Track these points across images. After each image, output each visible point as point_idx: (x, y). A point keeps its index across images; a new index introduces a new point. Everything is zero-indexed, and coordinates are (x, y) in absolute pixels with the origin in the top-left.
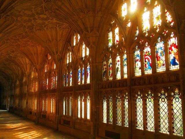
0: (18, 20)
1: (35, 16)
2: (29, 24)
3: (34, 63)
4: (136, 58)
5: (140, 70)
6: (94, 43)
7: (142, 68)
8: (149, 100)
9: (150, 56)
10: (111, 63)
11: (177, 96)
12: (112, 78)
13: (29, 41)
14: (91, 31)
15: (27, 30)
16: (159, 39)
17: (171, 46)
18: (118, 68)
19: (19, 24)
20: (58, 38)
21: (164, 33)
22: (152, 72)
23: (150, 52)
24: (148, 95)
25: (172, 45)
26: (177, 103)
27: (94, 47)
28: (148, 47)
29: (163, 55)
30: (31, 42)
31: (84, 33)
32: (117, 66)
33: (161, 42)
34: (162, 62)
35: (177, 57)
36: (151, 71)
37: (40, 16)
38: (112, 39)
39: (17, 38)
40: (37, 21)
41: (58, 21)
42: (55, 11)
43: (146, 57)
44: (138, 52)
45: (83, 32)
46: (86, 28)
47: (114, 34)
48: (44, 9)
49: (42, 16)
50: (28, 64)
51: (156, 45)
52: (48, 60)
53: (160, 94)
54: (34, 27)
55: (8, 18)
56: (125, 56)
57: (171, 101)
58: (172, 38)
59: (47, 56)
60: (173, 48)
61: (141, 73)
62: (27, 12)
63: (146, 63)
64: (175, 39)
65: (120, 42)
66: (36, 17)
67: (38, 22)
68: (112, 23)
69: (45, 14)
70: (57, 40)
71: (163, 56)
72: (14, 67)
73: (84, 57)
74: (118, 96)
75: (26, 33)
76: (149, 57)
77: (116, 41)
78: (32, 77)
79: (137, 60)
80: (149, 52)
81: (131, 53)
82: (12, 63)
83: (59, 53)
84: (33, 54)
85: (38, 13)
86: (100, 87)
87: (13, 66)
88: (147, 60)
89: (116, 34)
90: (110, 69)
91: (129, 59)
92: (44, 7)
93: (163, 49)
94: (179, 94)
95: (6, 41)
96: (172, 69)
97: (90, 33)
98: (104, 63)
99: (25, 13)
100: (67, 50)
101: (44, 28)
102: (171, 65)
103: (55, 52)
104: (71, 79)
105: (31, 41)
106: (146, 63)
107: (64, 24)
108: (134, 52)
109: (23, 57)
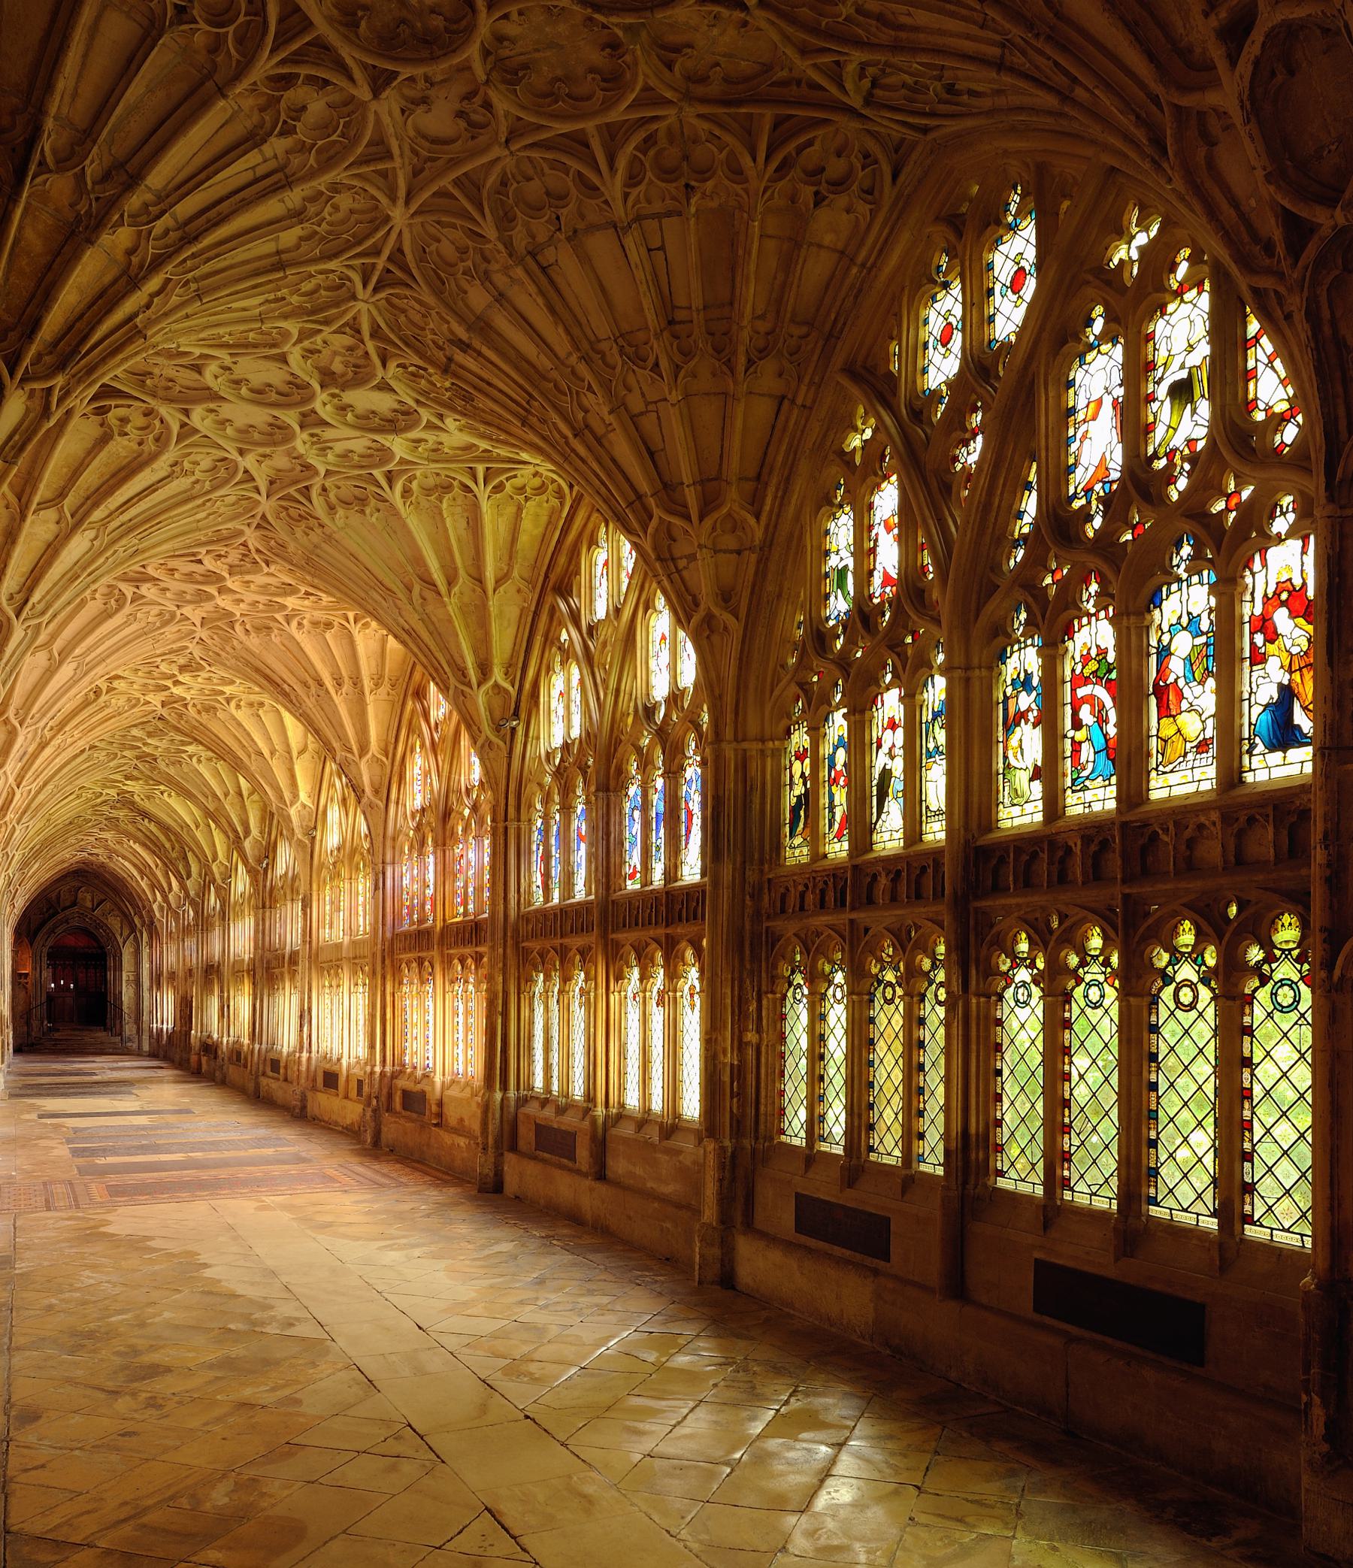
2: (281, 461)
3: (336, 745)
4: (1012, 703)
5: (1037, 787)
6: (726, 597)
7: (1047, 772)
8: (1086, 996)
9: (1109, 686)
10: (841, 737)
11: (1286, 970)
12: (846, 845)
13: (288, 590)
14: (708, 505)
15: (267, 506)
16: (1186, 550)
17: (1272, 601)
18: (886, 774)
19: (206, 463)
20: (490, 575)
21: (1220, 506)
22: (1119, 799)
23: (1111, 657)
24: (1083, 964)
25: (1277, 594)
26: (1286, 1021)
28: (1102, 614)
29: (1207, 672)
30: (307, 593)
32: (880, 761)
33: (1195, 579)
34: (1191, 725)
35: (1307, 688)
36: (1112, 791)
37: (351, 397)
38: (850, 562)
39: (209, 563)
40: (329, 434)
41: (483, 436)
42: (450, 359)
43: (1081, 692)
44: (1026, 659)
45: (651, 517)
46: (668, 488)
47: (863, 528)
48: (371, 346)
49: (363, 399)
50: (300, 753)
51: (1155, 601)
52: (428, 721)
53: (1166, 957)
54: (317, 483)
55: (122, 412)
56: (937, 691)
57: (1238, 1002)
58: (1279, 540)
59: (420, 694)
60: (1281, 618)
61: (1040, 805)
62: (258, 371)
63: (1080, 735)
64: (1304, 552)
65: (910, 581)
66: (322, 404)
67: (339, 448)
68: (855, 442)
69: (384, 387)
70: (480, 580)
71: (1202, 683)
72: (207, 775)
73: (667, 701)
74: (882, 969)
75: (263, 524)
76: (1101, 692)
77: (877, 579)
78: (332, 838)
79: (1021, 716)
80: (1103, 652)
81: (975, 661)
82: (191, 749)
83: (498, 675)
84: (329, 683)
85: (328, 378)
87: (201, 768)
88: (1086, 714)
89: (880, 530)
90: (834, 782)
91: (958, 711)
93: (1205, 625)
94: (1300, 960)
95: (128, 590)
96: (1262, 776)
97: (695, 517)
98: (795, 738)
100: (554, 649)
101: (387, 493)
102: (1260, 748)
104: (581, 855)
105: (303, 589)
106: (1080, 735)
107: (525, 456)
108: (1002, 658)
109: (261, 704)
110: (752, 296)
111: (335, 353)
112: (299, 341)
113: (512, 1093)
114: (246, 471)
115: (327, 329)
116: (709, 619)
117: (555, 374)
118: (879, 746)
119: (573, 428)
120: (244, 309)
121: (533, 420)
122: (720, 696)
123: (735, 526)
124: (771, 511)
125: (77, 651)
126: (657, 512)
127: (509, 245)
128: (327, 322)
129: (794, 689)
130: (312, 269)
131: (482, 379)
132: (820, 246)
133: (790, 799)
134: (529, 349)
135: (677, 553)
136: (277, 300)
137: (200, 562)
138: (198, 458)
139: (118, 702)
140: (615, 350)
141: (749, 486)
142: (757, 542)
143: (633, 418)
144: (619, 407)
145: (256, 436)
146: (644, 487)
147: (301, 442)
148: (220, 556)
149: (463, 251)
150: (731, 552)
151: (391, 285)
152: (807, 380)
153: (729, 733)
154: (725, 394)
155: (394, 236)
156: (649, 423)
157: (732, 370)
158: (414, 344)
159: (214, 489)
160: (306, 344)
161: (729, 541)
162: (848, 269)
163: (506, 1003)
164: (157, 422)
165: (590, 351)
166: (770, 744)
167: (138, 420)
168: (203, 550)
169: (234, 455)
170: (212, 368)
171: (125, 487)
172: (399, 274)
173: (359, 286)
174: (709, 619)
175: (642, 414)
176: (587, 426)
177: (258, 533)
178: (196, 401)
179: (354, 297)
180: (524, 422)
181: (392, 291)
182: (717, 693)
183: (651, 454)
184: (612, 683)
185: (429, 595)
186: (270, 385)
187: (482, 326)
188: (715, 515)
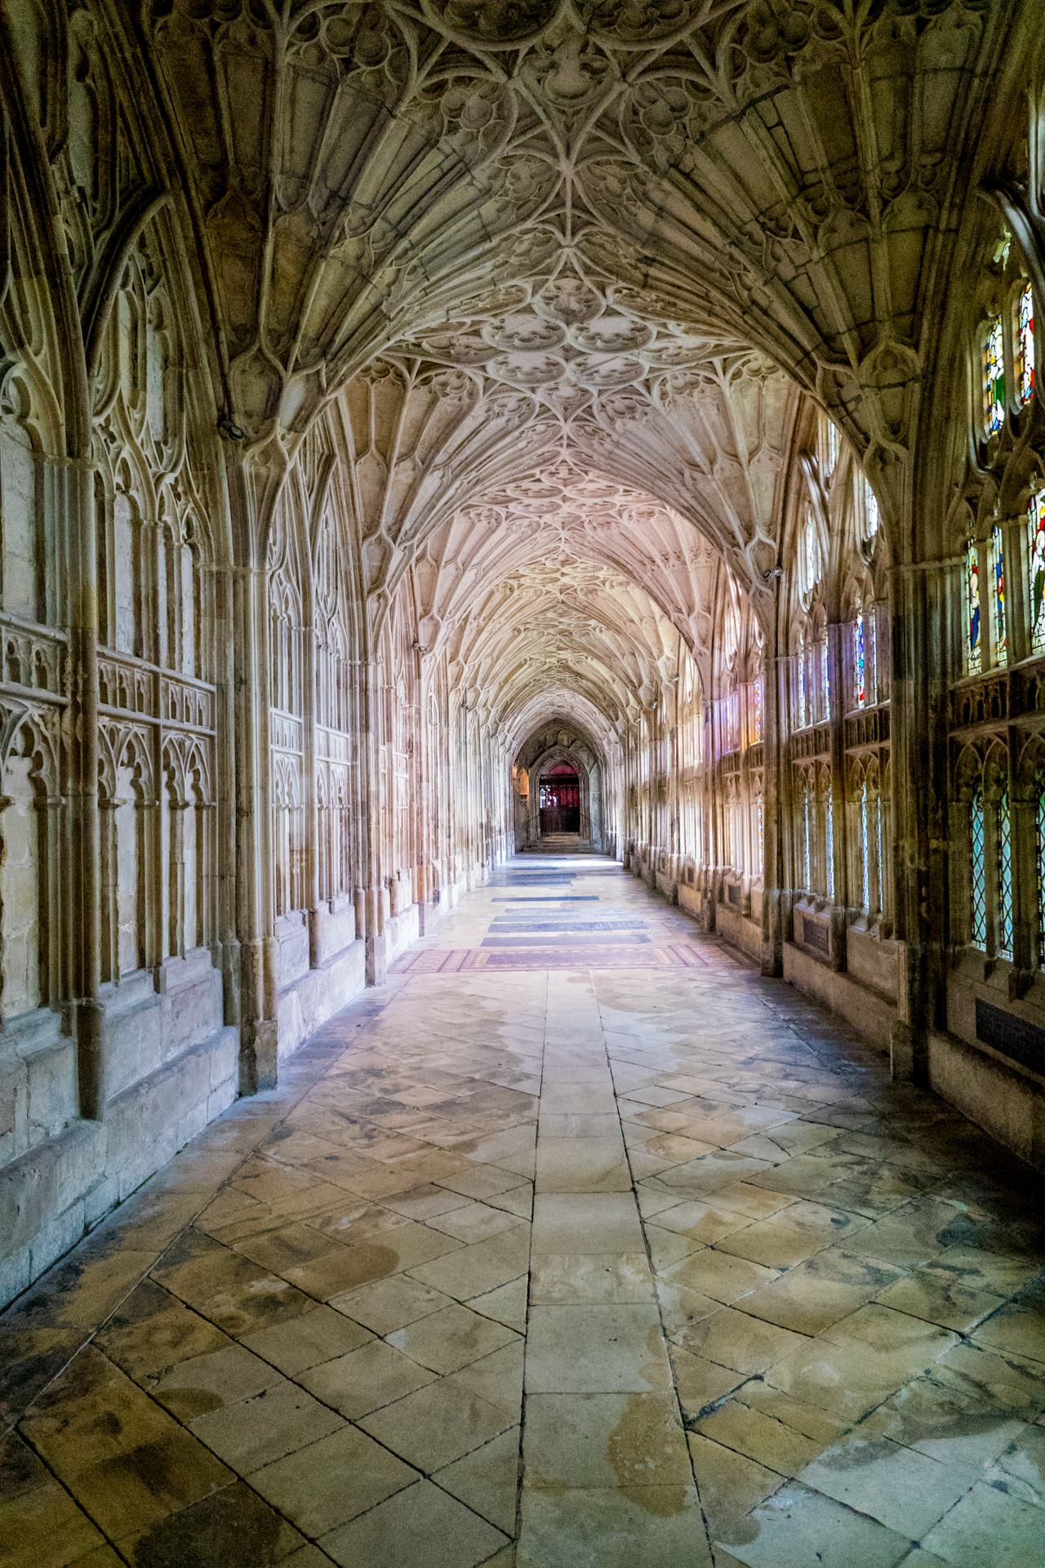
0: (495, 381)
1: (561, 338)
6: (895, 429)
19: (512, 404)
27: (897, 458)
31: (819, 375)
39: (547, 482)
42: (646, 276)
46: (828, 340)
48: (588, 282)
55: (442, 378)
69: (610, 312)
85: (570, 316)
86: (949, 714)
92: (577, 267)
97: (854, 362)
99: (508, 332)
103: (735, 526)
110: (874, 139)
111: (570, 295)
112: (534, 293)
113: (788, 891)
114: (542, 405)
115: (552, 278)
116: (880, 453)
117: (717, 265)
118: (1035, 549)
119: (741, 307)
120: (479, 278)
121: (717, 309)
122: (897, 523)
123: (898, 361)
124: (929, 340)
125: (475, 561)
126: (820, 364)
127: (653, 166)
128: (549, 271)
129: (965, 506)
130: (516, 231)
131: (673, 285)
132: (936, 71)
133: (968, 614)
134: (695, 249)
135: (846, 396)
136: (503, 264)
137: (539, 480)
138: (505, 401)
139: (528, 595)
140: (758, 227)
141: (906, 321)
142: (919, 371)
143: (787, 284)
144: (772, 277)
145: (539, 375)
146: (808, 347)
147: (570, 369)
148: (552, 474)
149: (622, 182)
150: (895, 386)
151: (582, 228)
152: (946, 205)
153: (907, 556)
154: (866, 240)
155: (569, 185)
156: (802, 286)
157: (868, 215)
158: (616, 271)
159: (522, 422)
160: (542, 292)
161: (891, 376)
162: (970, 83)
163: (779, 813)
164: (467, 381)
165: (738, 238)
166: (947, 562)
167: (455, 382)
168: (537, 471)
169: (529, 394)
170: (486, 330)
171: (455, 434)
172: (584, 216)
173: (558, 235)
174: (880, 453)
175: (794, 278)
176: (754, 302)
177: (571, 450)
178: (489, 358)
179: (560, 246)
180: (710, 313)
181: (585, 231)
182: (894, 520)
183: (807, 311)
184: (837, 526)
185: (697, 475)
186: (534, 333)
187: (655, 239)
188: (872, 355)
